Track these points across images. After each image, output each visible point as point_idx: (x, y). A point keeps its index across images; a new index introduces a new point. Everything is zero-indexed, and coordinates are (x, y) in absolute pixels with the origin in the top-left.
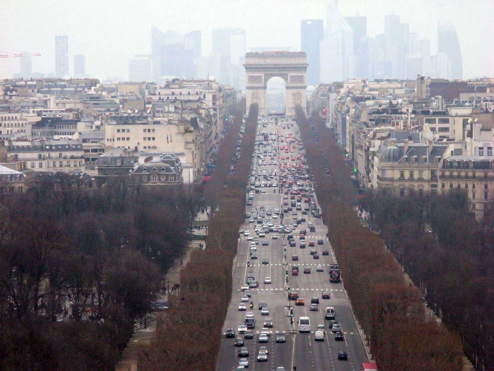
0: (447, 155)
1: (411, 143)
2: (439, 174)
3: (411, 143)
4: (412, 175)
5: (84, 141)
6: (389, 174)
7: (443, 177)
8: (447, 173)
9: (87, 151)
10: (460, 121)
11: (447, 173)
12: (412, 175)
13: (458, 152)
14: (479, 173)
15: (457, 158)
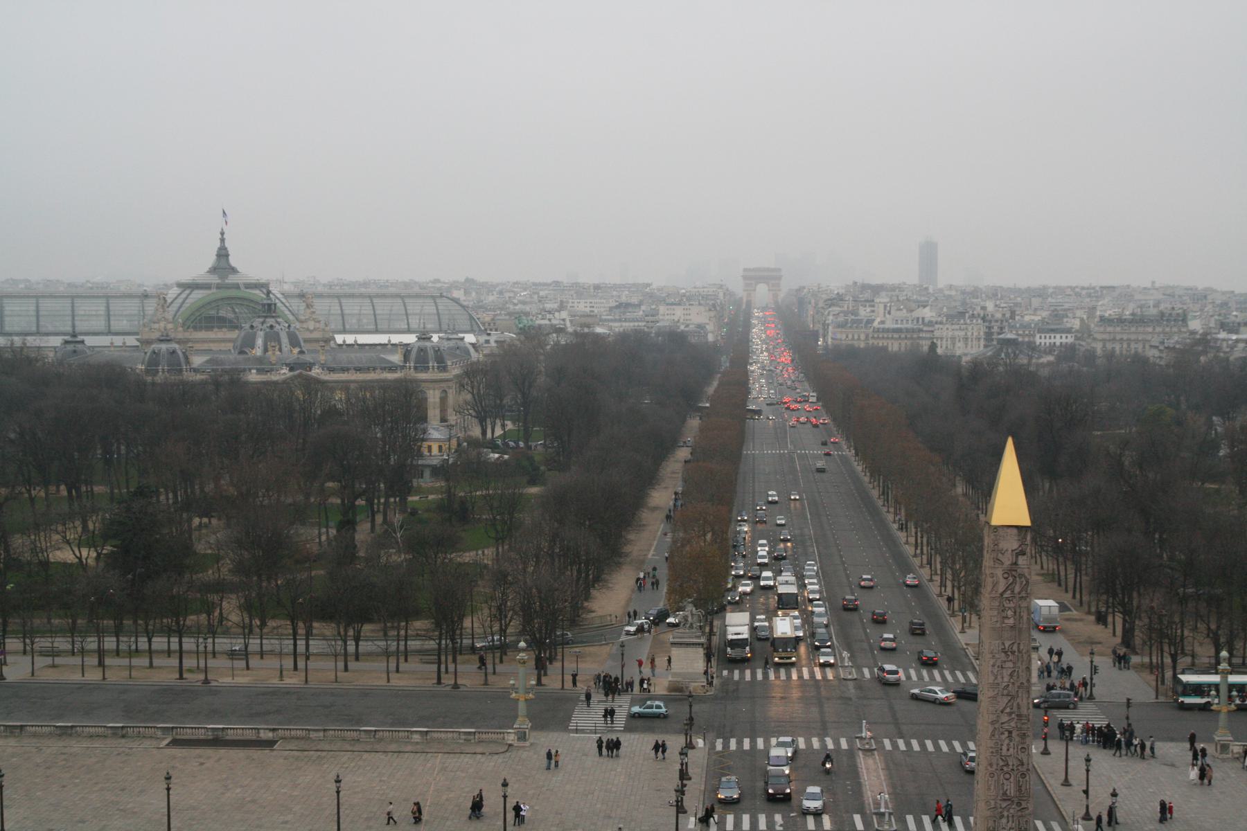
0: (876, 324)
1: (853, 317)
2: (871, 336)
3: (853, 317)
4: (853, 336)
5: (646, 316)
6: (839, 336)
7: (873, 337)
8: (876, 336)
9: (648, 322)
10: (882, 306)
11: (876, 336)
12: (853, 336)
13: (882, 322)
14: (896, 336)
15: (882, 326)
